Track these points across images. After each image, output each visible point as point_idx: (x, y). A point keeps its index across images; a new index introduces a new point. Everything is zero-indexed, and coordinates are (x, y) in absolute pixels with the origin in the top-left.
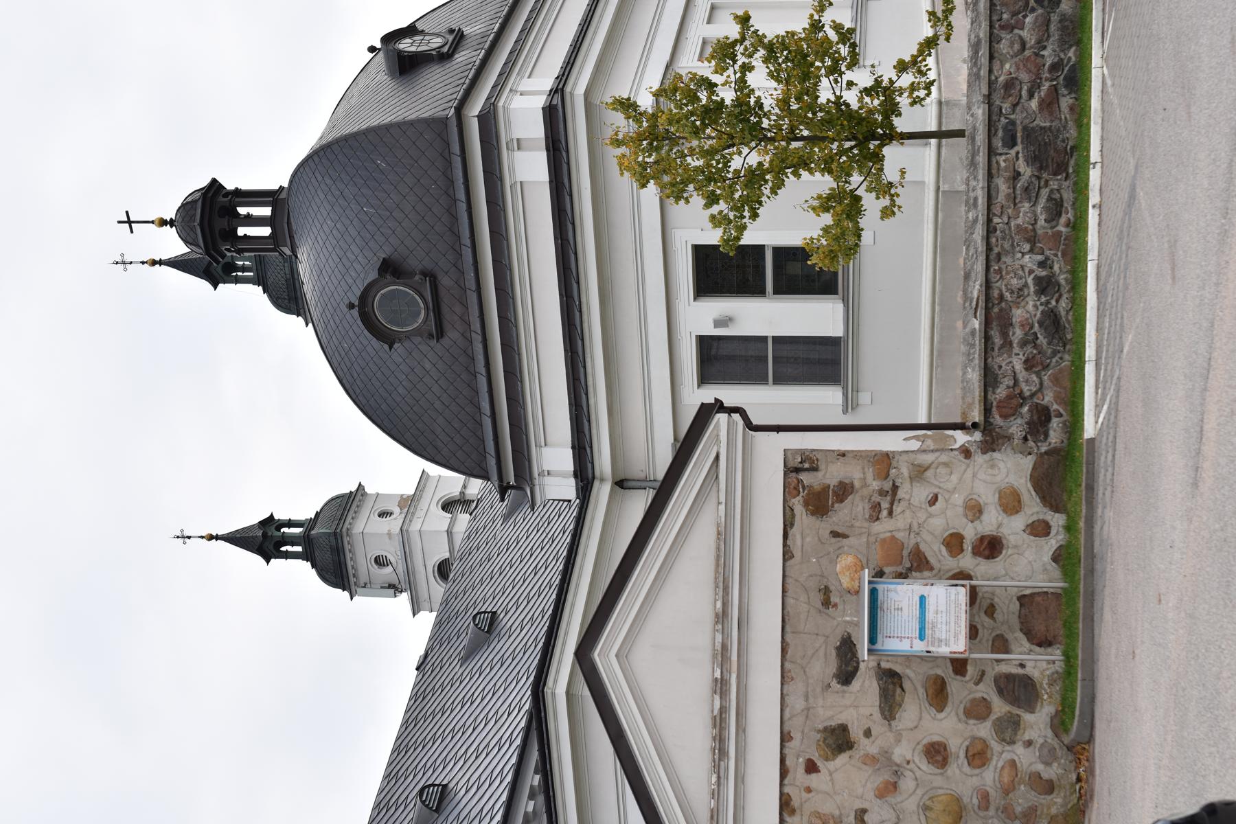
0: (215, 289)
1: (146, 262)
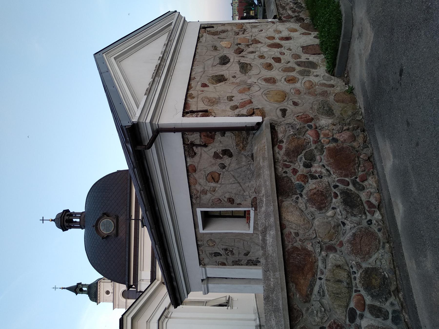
0: (76, 295)
1: (61, 288)
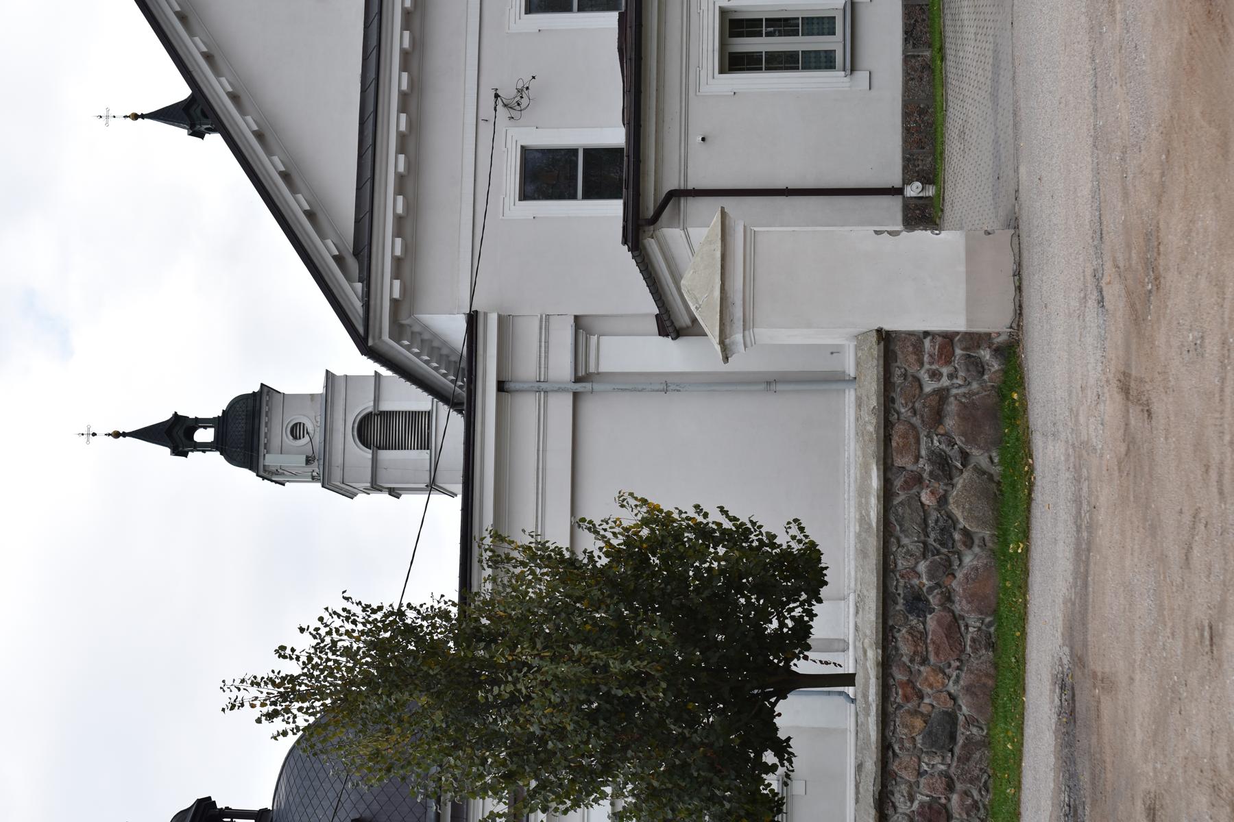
1: (129, 117)
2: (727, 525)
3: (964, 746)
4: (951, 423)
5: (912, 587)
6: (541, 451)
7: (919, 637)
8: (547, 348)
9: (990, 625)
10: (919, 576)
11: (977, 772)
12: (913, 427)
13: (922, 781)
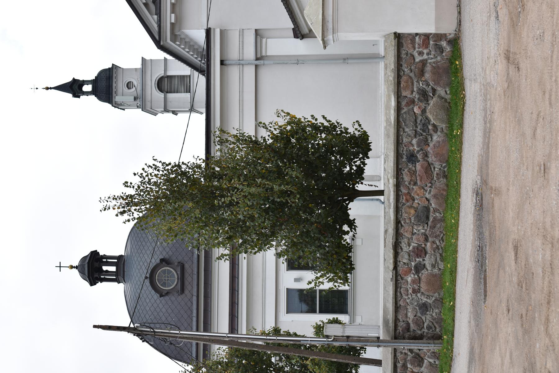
2: (326, 124)
3: (433, 221)
4: (428, 76)
5: (410, 150)
6: (241, 92)
7: (413, 173)
8: (243, 44)
9: (444, 167)
10: (413, 145)
11: (438, 233)
12: (411, 77)
13: (414, 237)
